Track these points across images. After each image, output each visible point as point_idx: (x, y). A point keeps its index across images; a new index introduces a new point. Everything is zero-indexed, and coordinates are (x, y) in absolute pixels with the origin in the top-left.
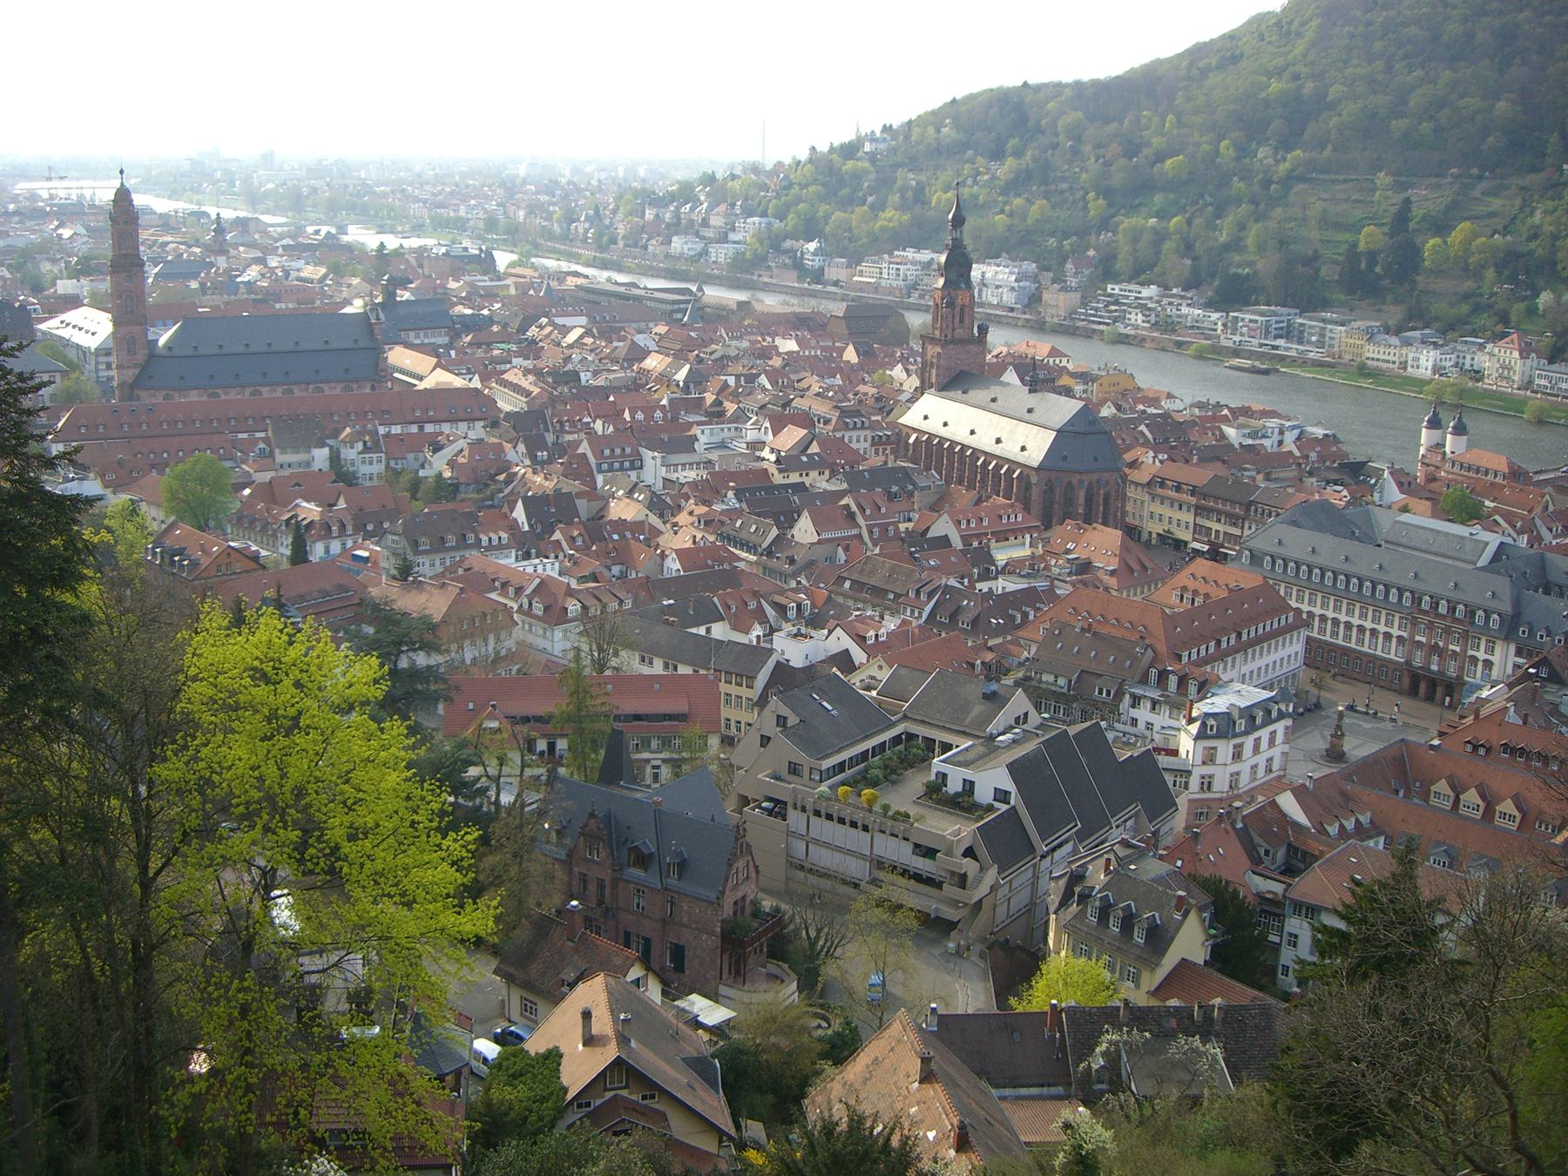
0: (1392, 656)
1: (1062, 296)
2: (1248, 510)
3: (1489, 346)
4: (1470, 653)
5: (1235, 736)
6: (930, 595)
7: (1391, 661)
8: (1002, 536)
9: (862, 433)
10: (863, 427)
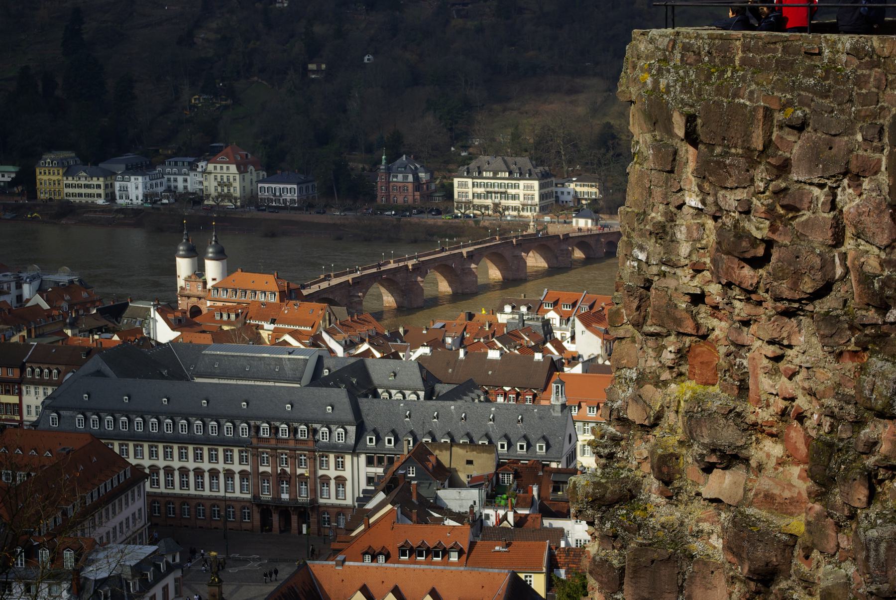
0: (237, 494)
2: (23, 370)
3: (202, 164)
4: (321, 472)
7: (237, 500)
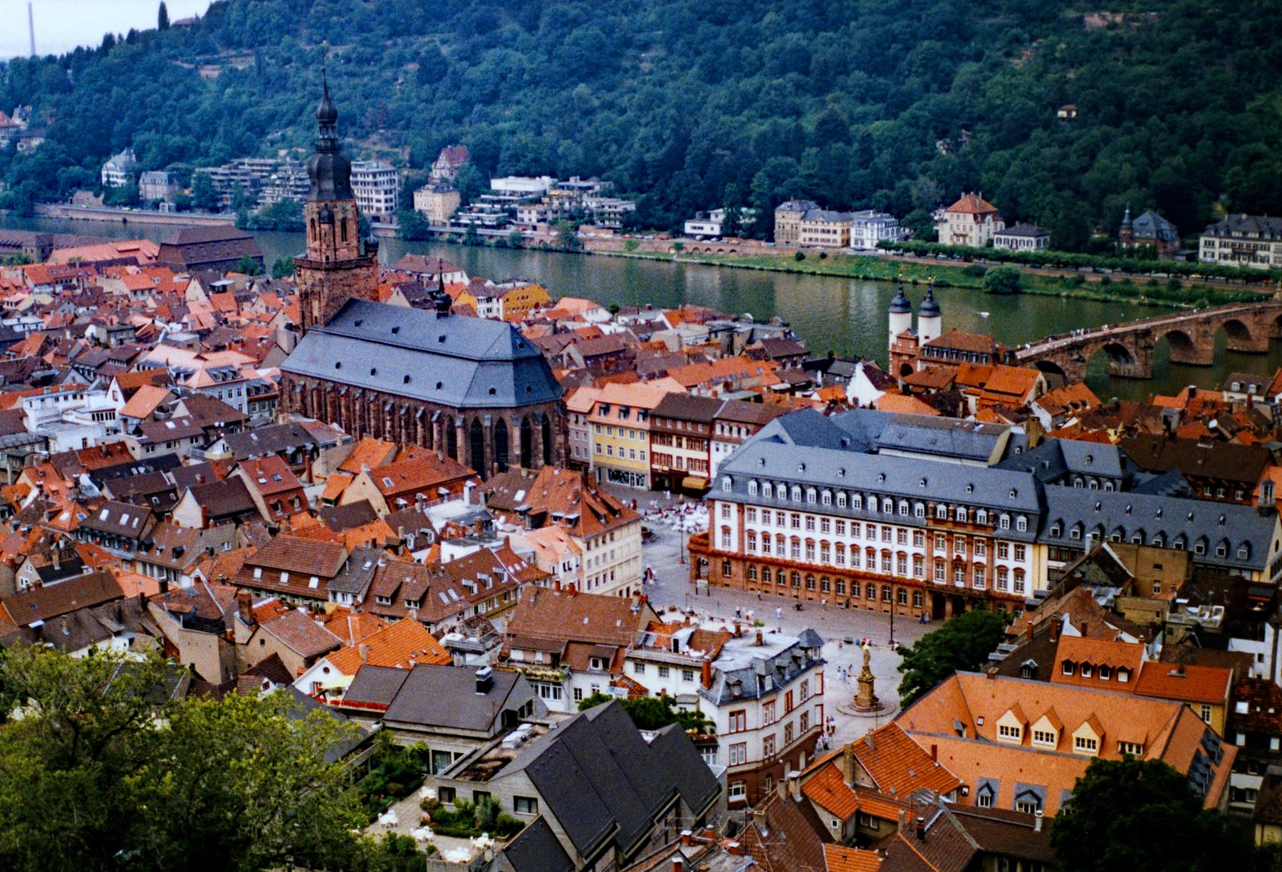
2: (712, 428)
4: (998, 562)
5: (764, 694)
8: (432, 493)
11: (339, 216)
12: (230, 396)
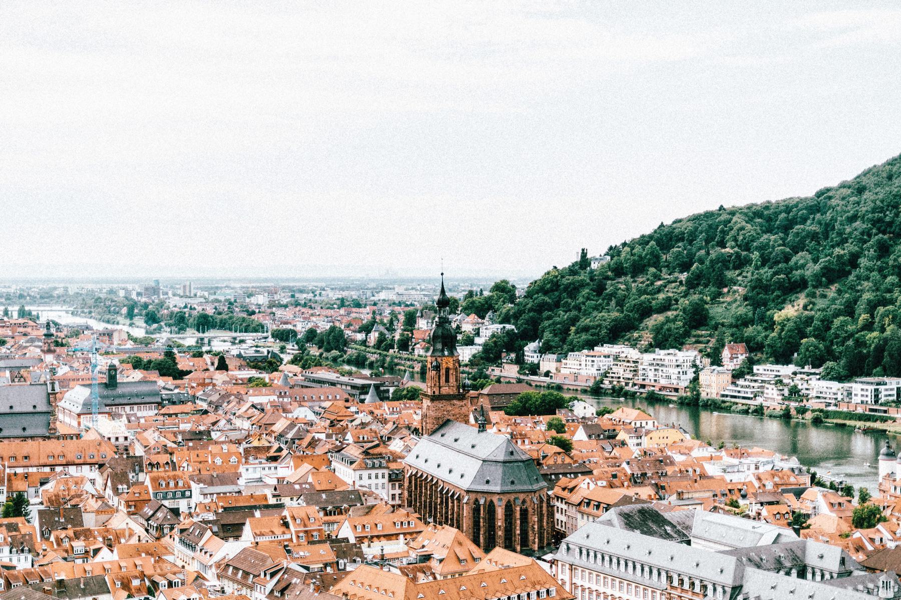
1: (714, 377)
6: (273, 575)
9: (380, 472)
10: (380, 467)
11: (444, 366)
12: (377, 477)
